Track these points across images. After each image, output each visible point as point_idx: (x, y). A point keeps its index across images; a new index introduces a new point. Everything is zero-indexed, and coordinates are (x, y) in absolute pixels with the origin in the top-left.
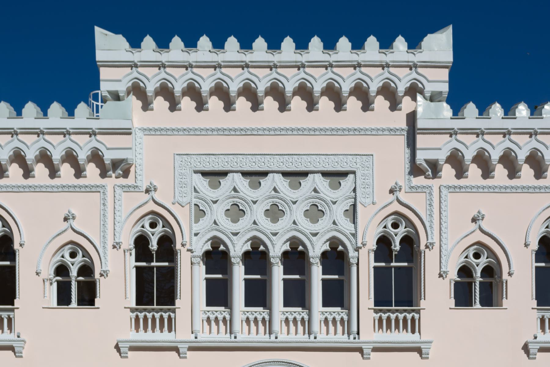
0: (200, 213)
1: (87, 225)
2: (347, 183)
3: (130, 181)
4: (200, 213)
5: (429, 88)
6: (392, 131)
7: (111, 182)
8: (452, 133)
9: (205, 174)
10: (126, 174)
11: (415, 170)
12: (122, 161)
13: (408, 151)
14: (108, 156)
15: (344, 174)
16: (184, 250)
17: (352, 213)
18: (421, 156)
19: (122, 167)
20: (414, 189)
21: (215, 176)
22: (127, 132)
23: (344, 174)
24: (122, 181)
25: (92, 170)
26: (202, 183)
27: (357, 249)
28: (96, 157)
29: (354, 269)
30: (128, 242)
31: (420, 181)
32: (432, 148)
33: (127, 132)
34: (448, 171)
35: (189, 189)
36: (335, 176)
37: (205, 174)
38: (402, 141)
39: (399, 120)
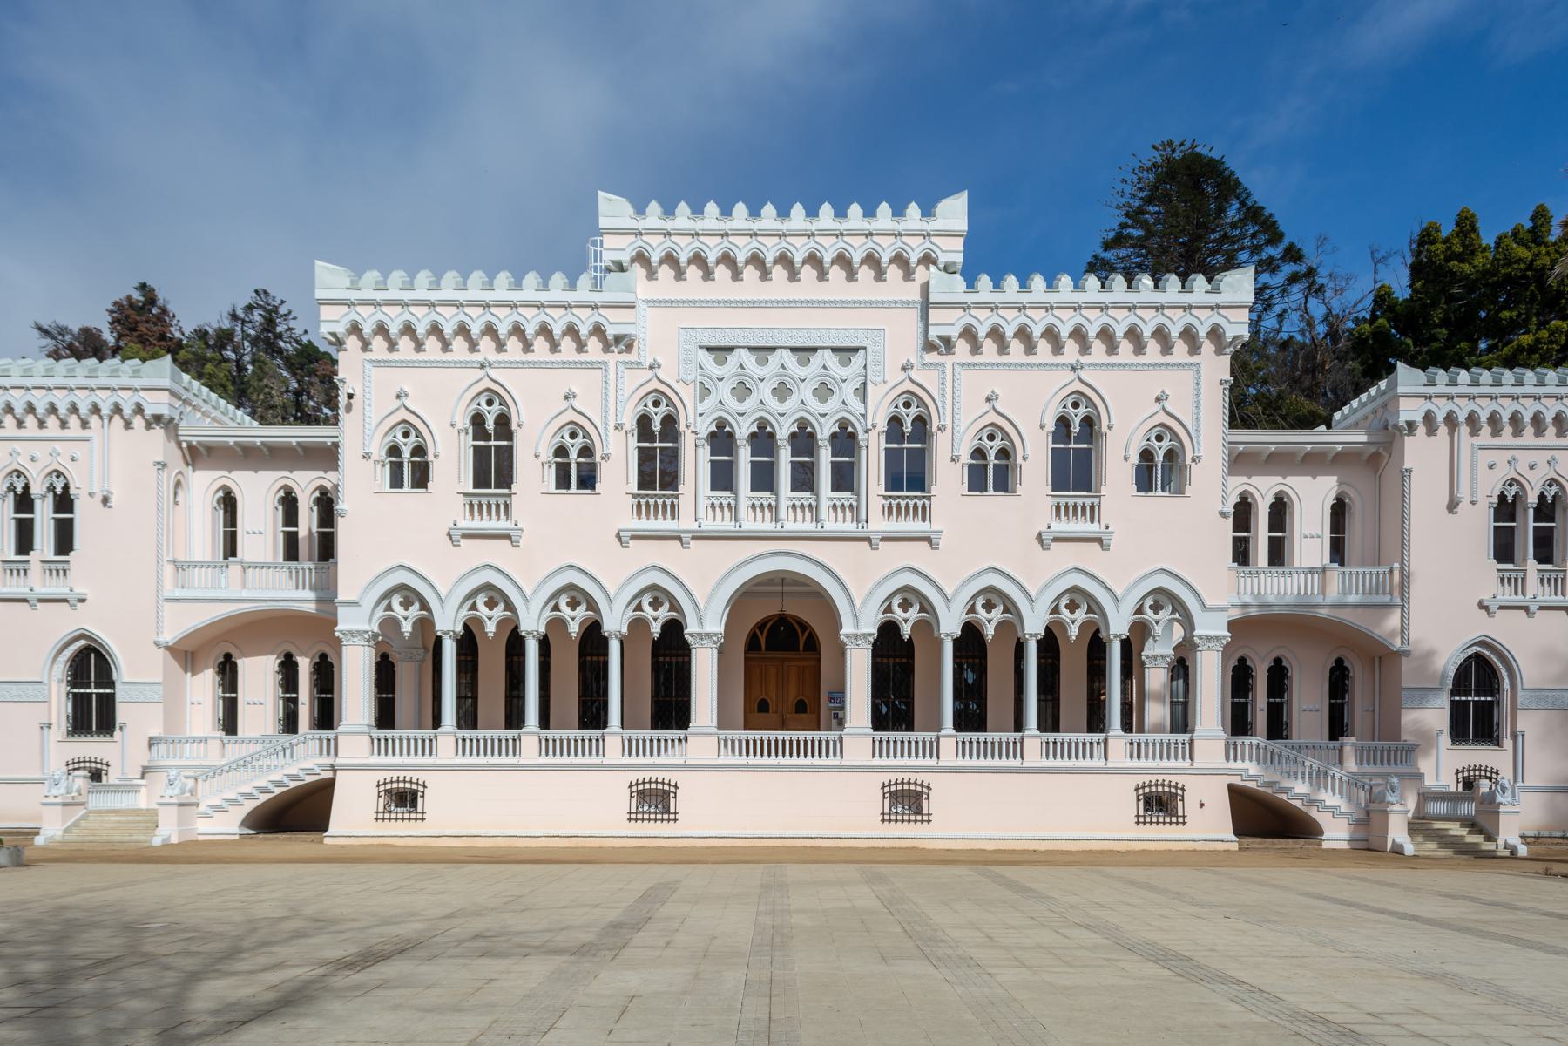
0: (705, 392)
1: (588, 404)
2: (857, 360)
3: (632, 357)
4: (705, 392)
5: (943, 259)
6: (905, 304)
7: (613, 358)
8: (966, 307)
9: (710, 349)
10: (629, 348)
11: (929, 347)
12: (625, 336)
13: (921, 325)
14: (611, 332)
15: (855, 350)
16: (688, 432)
17: (862, 392)
18: (934, 332)
19: (624, 342)
20: (926, 367)
21: (721, 351)
22: (630, 306)
23: (855, 350)
24: (625, 357)
25: (594, 344)
26: (707, 359)
27: (867, 431)
28: (598, 331)
29: (864, 452)
30: (630, 423)
31: (932, 357)
32: (946, 323)
33: (630, 306)
34: (962, 347)
35: (694, 366)
36: (845, 352)
37: (710, 349)
38: (914, 314)
39: (912, 292)
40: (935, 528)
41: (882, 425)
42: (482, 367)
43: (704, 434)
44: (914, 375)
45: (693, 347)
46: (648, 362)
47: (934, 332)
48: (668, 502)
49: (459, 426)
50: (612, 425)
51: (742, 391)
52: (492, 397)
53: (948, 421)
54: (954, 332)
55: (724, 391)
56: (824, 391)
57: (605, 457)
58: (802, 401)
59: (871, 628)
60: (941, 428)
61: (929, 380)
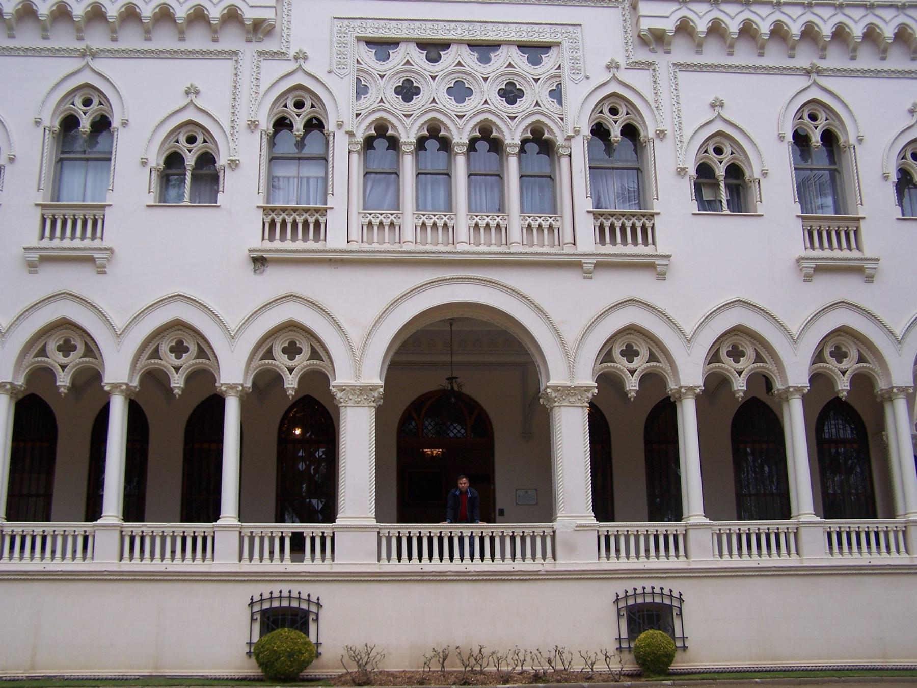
9: (370, 43)
12: (264, 20)
15: (546, 47)
17: (557, 94)
21: (383, 46)
23: (546, 47)
27: (569, 138)
35: (351, 62)
36: (535, 50)
37: (370, 43)
40: (661, 251)
41: (586, 131)
42: (83, 55)
43: (360, 138)
44: (624, 75)
45: (351, 40)
46: (292, 53)
47: (645, 24)
48: (312, 220)
49: (47, 122)
50: (242, 122)
51: (408, 91)
52: (88, 94)
53: (667, 126)
54: (669, 25)
55: (383, 91)
56: (511, 94)
57: (234, 164)
58: (485, 98)
59: (586, 379)
60: (661, 134)
61: (640, 80)
